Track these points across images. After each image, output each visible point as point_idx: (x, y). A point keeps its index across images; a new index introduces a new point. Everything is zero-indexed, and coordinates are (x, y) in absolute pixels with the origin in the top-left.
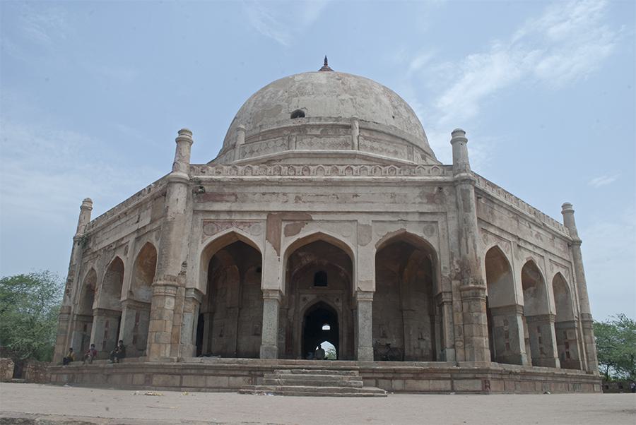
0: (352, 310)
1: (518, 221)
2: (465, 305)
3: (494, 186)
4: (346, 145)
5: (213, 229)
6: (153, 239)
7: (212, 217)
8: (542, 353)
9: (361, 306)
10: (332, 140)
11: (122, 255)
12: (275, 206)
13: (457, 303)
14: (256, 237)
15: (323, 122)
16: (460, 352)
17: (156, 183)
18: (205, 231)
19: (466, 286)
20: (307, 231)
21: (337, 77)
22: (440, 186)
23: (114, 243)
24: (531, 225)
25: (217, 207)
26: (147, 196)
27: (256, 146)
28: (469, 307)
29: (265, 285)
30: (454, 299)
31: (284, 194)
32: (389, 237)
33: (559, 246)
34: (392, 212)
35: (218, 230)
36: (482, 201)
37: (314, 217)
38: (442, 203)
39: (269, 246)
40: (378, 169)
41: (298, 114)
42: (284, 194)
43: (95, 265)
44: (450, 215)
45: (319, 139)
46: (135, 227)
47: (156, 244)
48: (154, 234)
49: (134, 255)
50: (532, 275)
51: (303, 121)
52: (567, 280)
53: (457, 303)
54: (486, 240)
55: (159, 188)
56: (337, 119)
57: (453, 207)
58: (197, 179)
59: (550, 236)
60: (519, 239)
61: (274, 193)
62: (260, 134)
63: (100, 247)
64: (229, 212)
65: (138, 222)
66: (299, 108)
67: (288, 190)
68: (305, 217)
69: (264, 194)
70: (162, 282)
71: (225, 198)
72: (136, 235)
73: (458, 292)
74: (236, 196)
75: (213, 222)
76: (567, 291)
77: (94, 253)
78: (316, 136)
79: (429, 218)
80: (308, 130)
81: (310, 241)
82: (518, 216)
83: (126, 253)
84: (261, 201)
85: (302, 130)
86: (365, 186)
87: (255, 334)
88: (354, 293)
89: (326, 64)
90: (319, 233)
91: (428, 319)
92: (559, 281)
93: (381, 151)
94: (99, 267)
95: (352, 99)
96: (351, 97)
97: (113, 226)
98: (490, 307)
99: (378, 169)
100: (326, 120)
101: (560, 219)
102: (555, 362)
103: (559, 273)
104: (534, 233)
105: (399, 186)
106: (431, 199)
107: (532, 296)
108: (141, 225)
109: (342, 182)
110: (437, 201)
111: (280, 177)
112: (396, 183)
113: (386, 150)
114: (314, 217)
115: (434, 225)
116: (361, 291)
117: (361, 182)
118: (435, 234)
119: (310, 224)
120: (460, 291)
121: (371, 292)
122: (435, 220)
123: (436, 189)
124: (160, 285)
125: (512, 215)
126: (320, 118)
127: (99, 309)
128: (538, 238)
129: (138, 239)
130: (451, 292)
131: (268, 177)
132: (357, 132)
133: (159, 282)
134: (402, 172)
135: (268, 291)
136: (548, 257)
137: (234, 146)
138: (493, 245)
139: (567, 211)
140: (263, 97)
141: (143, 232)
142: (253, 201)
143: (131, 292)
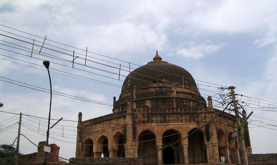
0: (178, 150)
2: (213, 147)
8: (235, 160)
9: (184, 149)
13: (211, 147)
16: (212, 160)
28: (214, 148)
53: (211, 147)
72: (112, 129)
87: (150, 158)
89: (157, 54)
91: (201, 151)
102: (239, 162)
120: (211, 144)
127: (96, 152)
129: (113, 130)
135: (159, 146)
143: (112, 147)
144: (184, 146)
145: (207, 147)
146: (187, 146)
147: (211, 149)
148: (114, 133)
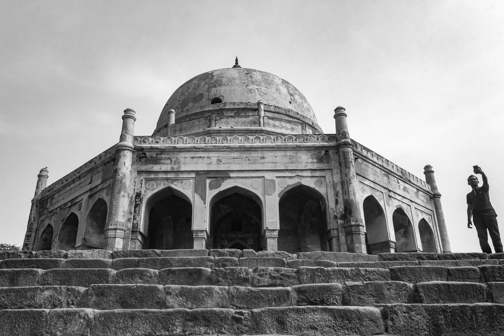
1: (388, 177)
3: (368, 150)
4: (255, 123)
5: (153, 185)
6: (104, 195)
7: (152, 176)
10: (244, 119)
11: (77, 210)
12: (202, 166)
13: (343, 238)
14: (186, 189)
15: (236, 107)
17: (106, 152)
18: (147, 186)
19: (349, 224)
20: (227, 185)
21: (246, 72)
22: (327, 149)
23: (69, 202)
24: (399, 181)
25: (156, 168)
26: (98, 162)
27: (184, 125)
29: (195, 227)
30: (340, 235)
31: (209, 158)
32: (289, 188)
33: (422, 198)
34: (291, 170)
35: (157, 186)
36: (360, 160)
37: (232, 175)
38: (328, 162)
39: (197, 197)
40: (279, 138)
41: (217, 100)
42: (209, 158)
43: (52, 221)
44: (335, 171)
45: (233, 119)
46: (89, 187)
47: (107, 199)
48: (105, 191)
49: (87, 209)
50: (401, 219)
51: (221, 106)
52: (431, 224)
54: (364, 191)
55: (108, 156)
56: (246, 104)
57: (337, 165)
58: (140, 147)
59: (415, 190)
60: (390, 191)
61: (200, 157)
62: (187, 116)
63: (56, 206)
64: (166, 172)
65: (90, 183)
66: (217, 96)
67: (211, 154)
68: (224, 175)
69: (193, 158)
70: (113, 227)
71: (163, 161)
72: (88, 194)
73: (343, 229)
74: (171, 160)
75: (153, 180)
76: (430, 232)
77: (50, 212)
78: (232, 117)
79: (317, 174)
80: (225, 112)
81: (228, 194)
82: (388, 173)
83: (79, 209)
84: (191, 164)
85: (221, 113)
86: (269, 151)
88: (263, 232)
90: (236, 187)
92: (423, 224)
93: (281, 128)
94: (56, 223)
96: (258, 87)
97: (68, 189)
98: (369, 243)
99: (279, 138)
100: (238, 105)
101: (423, 178)
103: (423, 219)
104: (402, 187)
105: (295, 150)
107: (402, 237)
108: (93, 185)
109: (252, 148)
110: (325, 161)
111: (205, 145)
112: (293, 148)
113: (285, 127)
114: (232, 175)
115: (323, 179)
116: (268, 230)
117: (266, 148)
118: (323, 185)
119: (228, 181)
121: (276, 230)
122: (323, 175)
123: (323, 152)
124: (111, 229)
125: (383, 173)
126: (234, 104)
128: (405, 191)
129: (90, 197)
130: (338, 229)
131: (195, 145)
132: (262, 113)
133: (110, 227)
134: (297, 140)
136: (413, 205)
137: (166, 126)
138: (369, 194)
139: (428, 171)
140: (188, 88)
141: (95, 191)
142: (185, 164)
143: (84, 239)
144: (268, 234)
145: (331, 239)
146: (276, 234)
147: (344, 243)
148: (92, 203)
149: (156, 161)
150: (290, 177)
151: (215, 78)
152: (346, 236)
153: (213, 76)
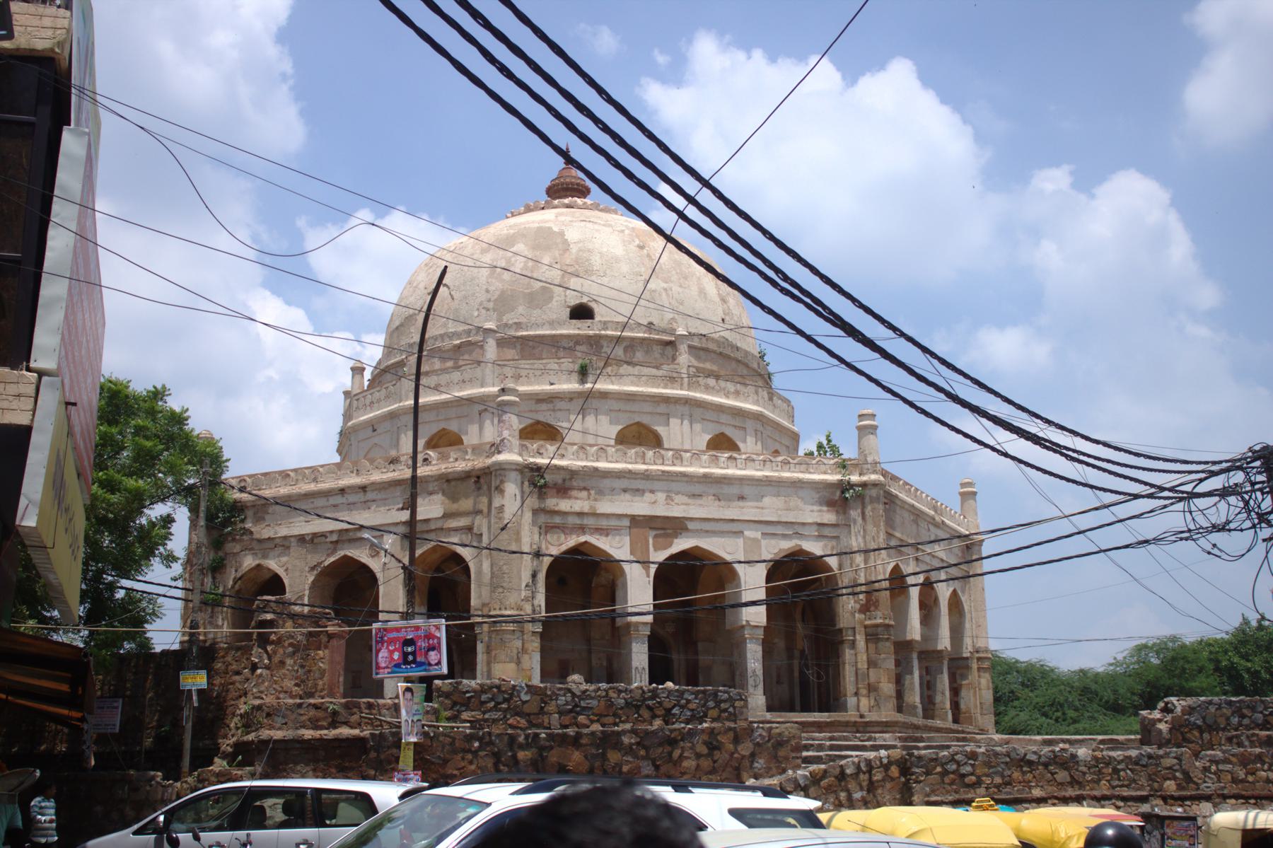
7: (557, 520)
14: (617, 547)
20: (682, 544)
37: (691, 525)
41: (581, 312)
71: (574, 493)
90: (697, 547)
95: (665, 290)
96: (665, 285)
106: (831, 504)
145: (842, 642)
146: (760, 634)
149: (563, 490)
150: (785, 536)
151: (574, 249)
152: (867, 641)
153: (566, 242)
